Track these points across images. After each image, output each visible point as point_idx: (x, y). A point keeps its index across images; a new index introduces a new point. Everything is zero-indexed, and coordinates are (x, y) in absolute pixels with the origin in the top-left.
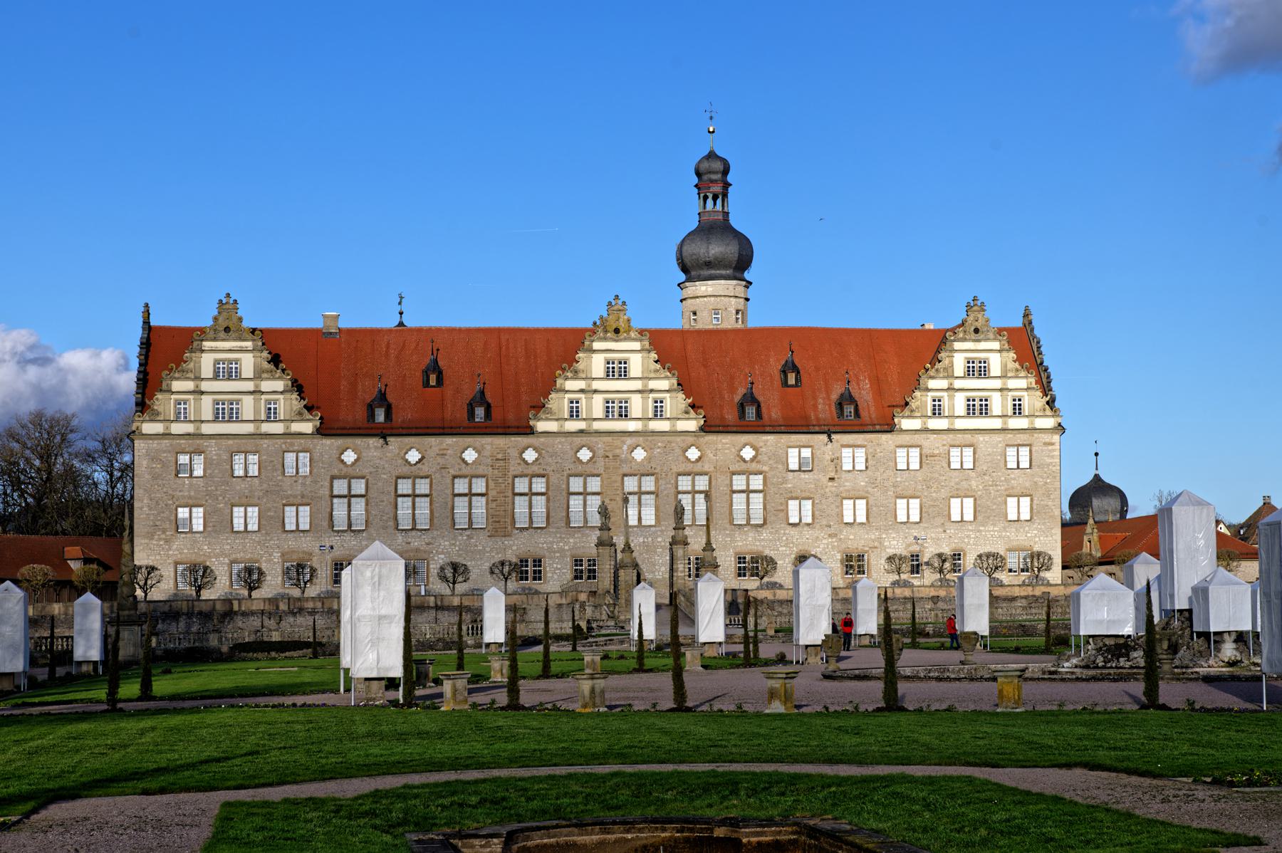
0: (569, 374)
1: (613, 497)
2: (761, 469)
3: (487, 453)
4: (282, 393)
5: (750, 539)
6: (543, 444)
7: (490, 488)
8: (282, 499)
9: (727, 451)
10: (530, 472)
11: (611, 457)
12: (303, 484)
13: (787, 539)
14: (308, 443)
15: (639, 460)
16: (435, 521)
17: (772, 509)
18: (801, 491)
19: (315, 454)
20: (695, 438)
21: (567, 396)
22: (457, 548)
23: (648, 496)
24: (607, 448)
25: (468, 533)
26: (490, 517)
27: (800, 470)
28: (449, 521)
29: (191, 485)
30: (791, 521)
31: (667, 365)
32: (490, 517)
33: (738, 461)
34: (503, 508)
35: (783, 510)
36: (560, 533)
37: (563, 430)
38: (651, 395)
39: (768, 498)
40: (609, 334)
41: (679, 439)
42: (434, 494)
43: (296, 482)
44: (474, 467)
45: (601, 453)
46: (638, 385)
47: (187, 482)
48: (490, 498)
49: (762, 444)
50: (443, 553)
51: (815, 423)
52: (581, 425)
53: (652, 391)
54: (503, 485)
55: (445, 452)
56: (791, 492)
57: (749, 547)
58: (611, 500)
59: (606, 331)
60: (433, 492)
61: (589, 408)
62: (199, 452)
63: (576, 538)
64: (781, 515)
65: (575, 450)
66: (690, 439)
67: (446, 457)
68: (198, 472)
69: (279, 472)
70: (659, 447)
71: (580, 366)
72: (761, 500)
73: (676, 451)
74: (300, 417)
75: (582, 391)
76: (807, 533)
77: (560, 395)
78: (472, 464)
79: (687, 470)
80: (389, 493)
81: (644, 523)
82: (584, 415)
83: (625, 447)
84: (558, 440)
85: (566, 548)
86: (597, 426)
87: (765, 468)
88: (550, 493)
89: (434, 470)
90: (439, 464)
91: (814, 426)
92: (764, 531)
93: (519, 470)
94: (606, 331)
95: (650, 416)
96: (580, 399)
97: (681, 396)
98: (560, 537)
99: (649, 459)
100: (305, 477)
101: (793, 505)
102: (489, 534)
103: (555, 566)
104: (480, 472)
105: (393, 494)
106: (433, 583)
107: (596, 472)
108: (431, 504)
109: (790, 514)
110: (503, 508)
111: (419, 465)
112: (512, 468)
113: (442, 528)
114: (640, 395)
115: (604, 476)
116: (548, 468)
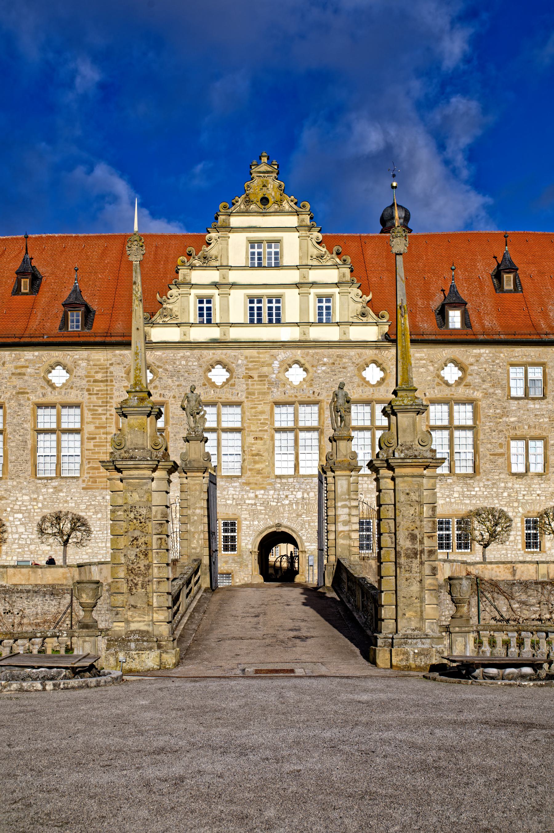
0: (197, 263)
1: (260, 435)
2: (469, 397)
3: (81, 372)
5: (456, 495)
6: (160, 359)
7: (86, 420)
9: (422, 370)
11: (256, 378)
13: (509, 495)
15: (296, 383)
16: (10, 465)
17: (488, 453)
18: (529, 427)
20: (377, 351)
21: (194, 292)
22: (40, 505)
23: (308, 435)
24: (250, 365)
25: (55, 483)
26: (85, 462)
27: (527, 396)
28: (29, 467)
30: (514, 470)
31: (335, 249)
32: (85, 462)
33: (439, 384)
35: (502, 455)
37: (188, 340)
38: (313, 291)
39: (481, 436)
40: (253, 207)
41: (353, 352)
42: (9, 430)
44: (63, 391)
45: (241, 371)
46: (294, 276)
48: (86, 436)
49: (472, 360)
50: (19, 511)
51: (548, 331)
52: (213, 333)
53: (314, 284)
54: (104, 417)
55: (23, 370)
56: (515, 428)
57: (455, 506)
58: (256, 438)
59: (248, 202)
60: (7, 426)
61: (226, 309)
64: (501, 460)
65: (205, 367)
66: (370, 353)
67: (26, 378)
70: (324, 364)
71: (213, 250)
72: (470, 441)
73: (349, 369)
75: (216, 285)
76: (538, 486)
77: (183, 290)
78: (61, 388)
79: (365, 397)
81: (302, 471)
82: (217, 318)
83: (276, 364)
84: (181, 353)
86: (235, 334)
87: (478, 395)
89: (8, 395)
90: (15, 387)
91: (546, 334)
92: (476, 483)
94: (248, 202)
95: (312, 320)
96: (212, 297)
97: (355, 291)
99: (310, 381)
101: (517, 447)
102: (84, 486)
104: (72, 398)
106: (7, 553)
107: (234, 399)
108: (4, 445)
109: (513, 459)
112: (116, 394)
113: (18, 476)
114: (297, 291)
115: (247, 404)
116: (167, 392)
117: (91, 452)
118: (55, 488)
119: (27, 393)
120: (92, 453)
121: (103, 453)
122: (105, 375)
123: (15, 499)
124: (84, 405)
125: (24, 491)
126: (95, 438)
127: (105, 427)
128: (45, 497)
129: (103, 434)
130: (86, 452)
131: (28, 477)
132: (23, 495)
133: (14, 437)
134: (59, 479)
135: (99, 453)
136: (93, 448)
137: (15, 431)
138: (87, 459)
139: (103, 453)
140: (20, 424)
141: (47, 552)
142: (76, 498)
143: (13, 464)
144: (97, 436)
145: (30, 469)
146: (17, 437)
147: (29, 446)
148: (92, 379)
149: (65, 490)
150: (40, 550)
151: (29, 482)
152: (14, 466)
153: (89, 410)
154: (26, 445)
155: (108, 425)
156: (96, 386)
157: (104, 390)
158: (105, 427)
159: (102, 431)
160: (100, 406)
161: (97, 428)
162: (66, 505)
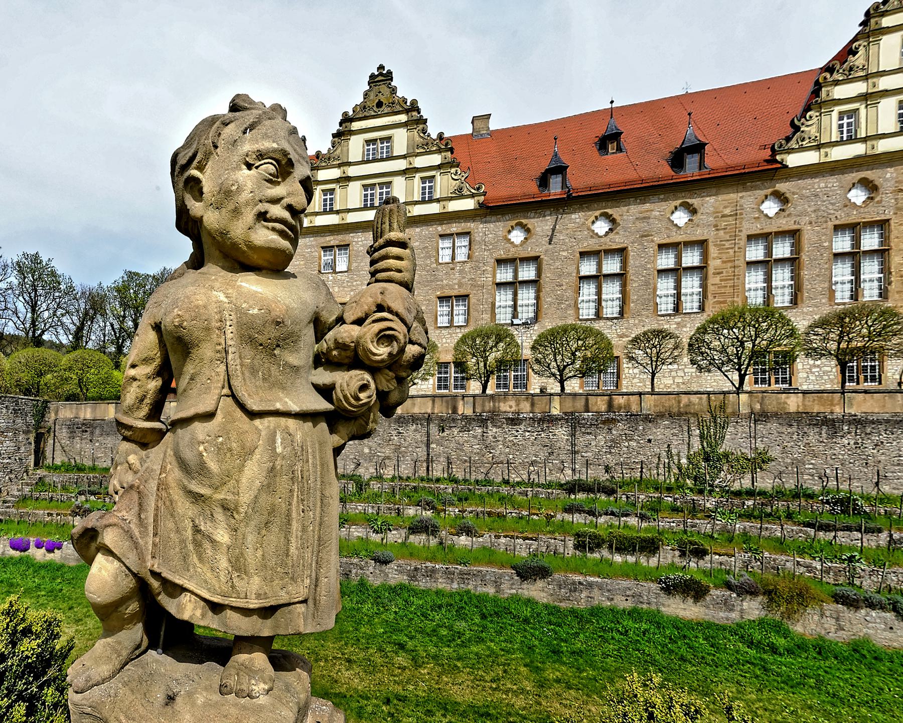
4: (439, 167)
8: (435, 290)
10: (777, 230)
12: (461, 272)
14: (470, 226)
16: (632, 305)
19: (476, 235)
29: (335, 281)
34: (731, 283)
43: (453, 269)
47: (331, 278)
52: (858, 149)
54: (731, 251)
62: (344, 247)
68: (342, 266)
69: (433, 260)
74: (459, 195)
80: (569, 274)
93: (756, 229)
100: (464, 262)
105: (574, 274)
110: (731, 283)
111: (611, 236)
118: (678, 324)
119: (652, 235)
120: (719, 288)
122: (735, 209)
124: (710, 241)
126: (722, 273)
135: (726, 286)
140: (642, 266)
144: (724, 271)
148: (720, 215)
149: (688, 325)
150: (661, 383)
153: (715, 245)
156: (724, 222)
157: (733, 224)
159: (730, 264)
160: (728, 240)
161: (724, 262)
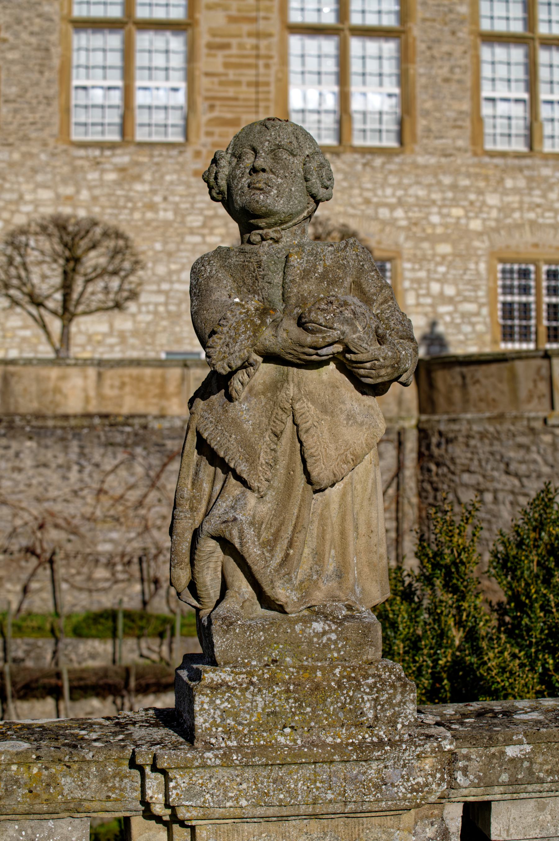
32: (201, 105)
34: (249, 75)
36: (456, 172)
48: (204, 39)
63: (505, 192)
85: (476, 225)
88: (416, 31)
98: (454, 187)
103: (435, 287)
110: (249, 75)
113: (25, 139)
117: (216, 80)
118: (122, 170)
121: (249, 84)
123: (15, 196)
125: (40, 178)
126: (226, 46)
127: (255, 20)
128: (97, 192)
129: (250, 35)
130: (203, 83)
131: (51, 142)
132: (39, 186)
133: (17, 35)
134: (132, 149)
135: (237, 83)
136: (221, 70)
137: (19, 22)
138: (207, 98)
139: (249, 84)
141: (99, 338)
142: (177, 199)
143: (11, 106)
144: (234, 42)
145: (56, 120)
146: (24, 36)
147: (56, 62)
149: (148, 177)
151: (53, 155)
152: (16, 111)
154: (48, 57)
155: (262, 14)
158: (255, 20)
159: (246, 28)
161: (232, 20)
162: (149, 215)
